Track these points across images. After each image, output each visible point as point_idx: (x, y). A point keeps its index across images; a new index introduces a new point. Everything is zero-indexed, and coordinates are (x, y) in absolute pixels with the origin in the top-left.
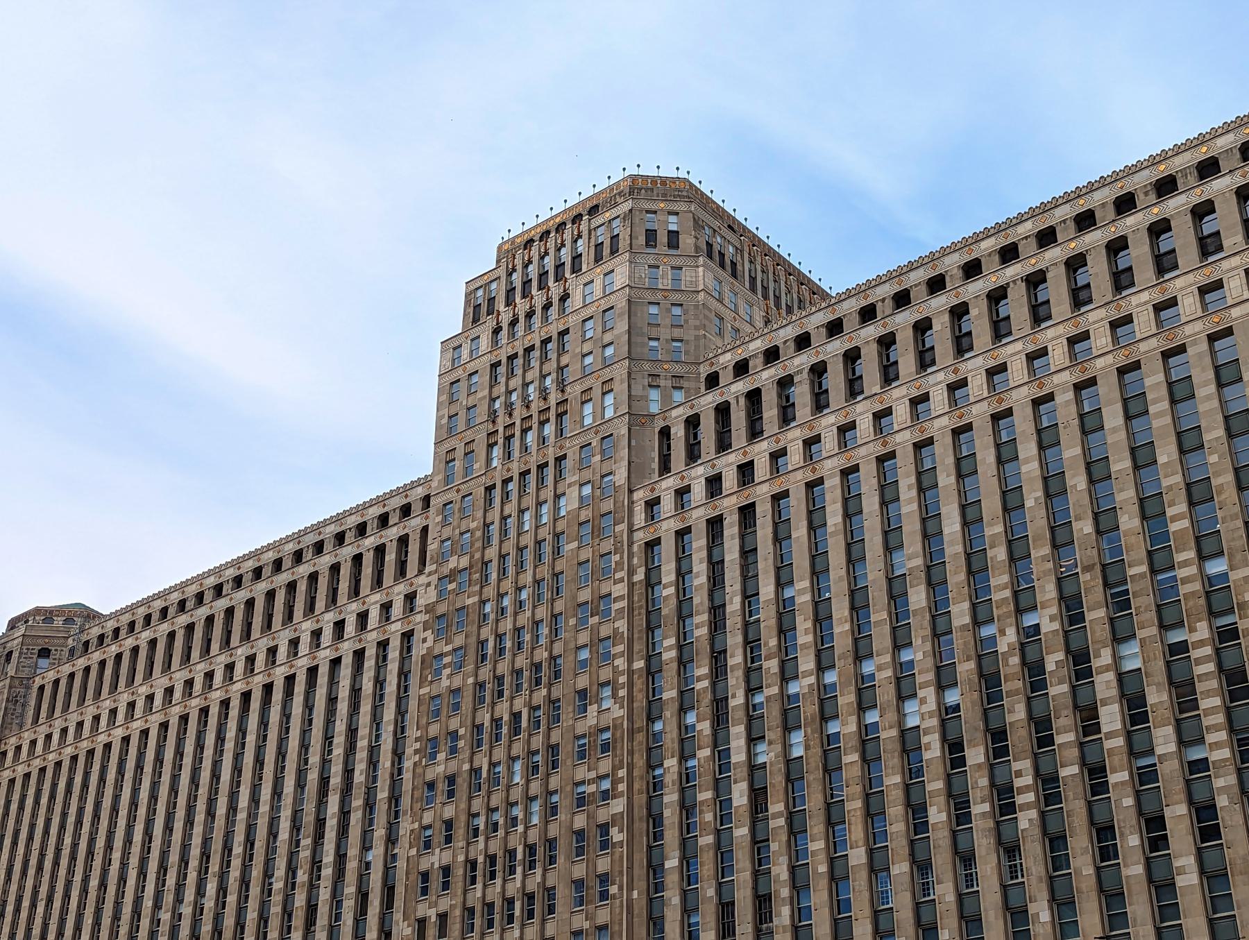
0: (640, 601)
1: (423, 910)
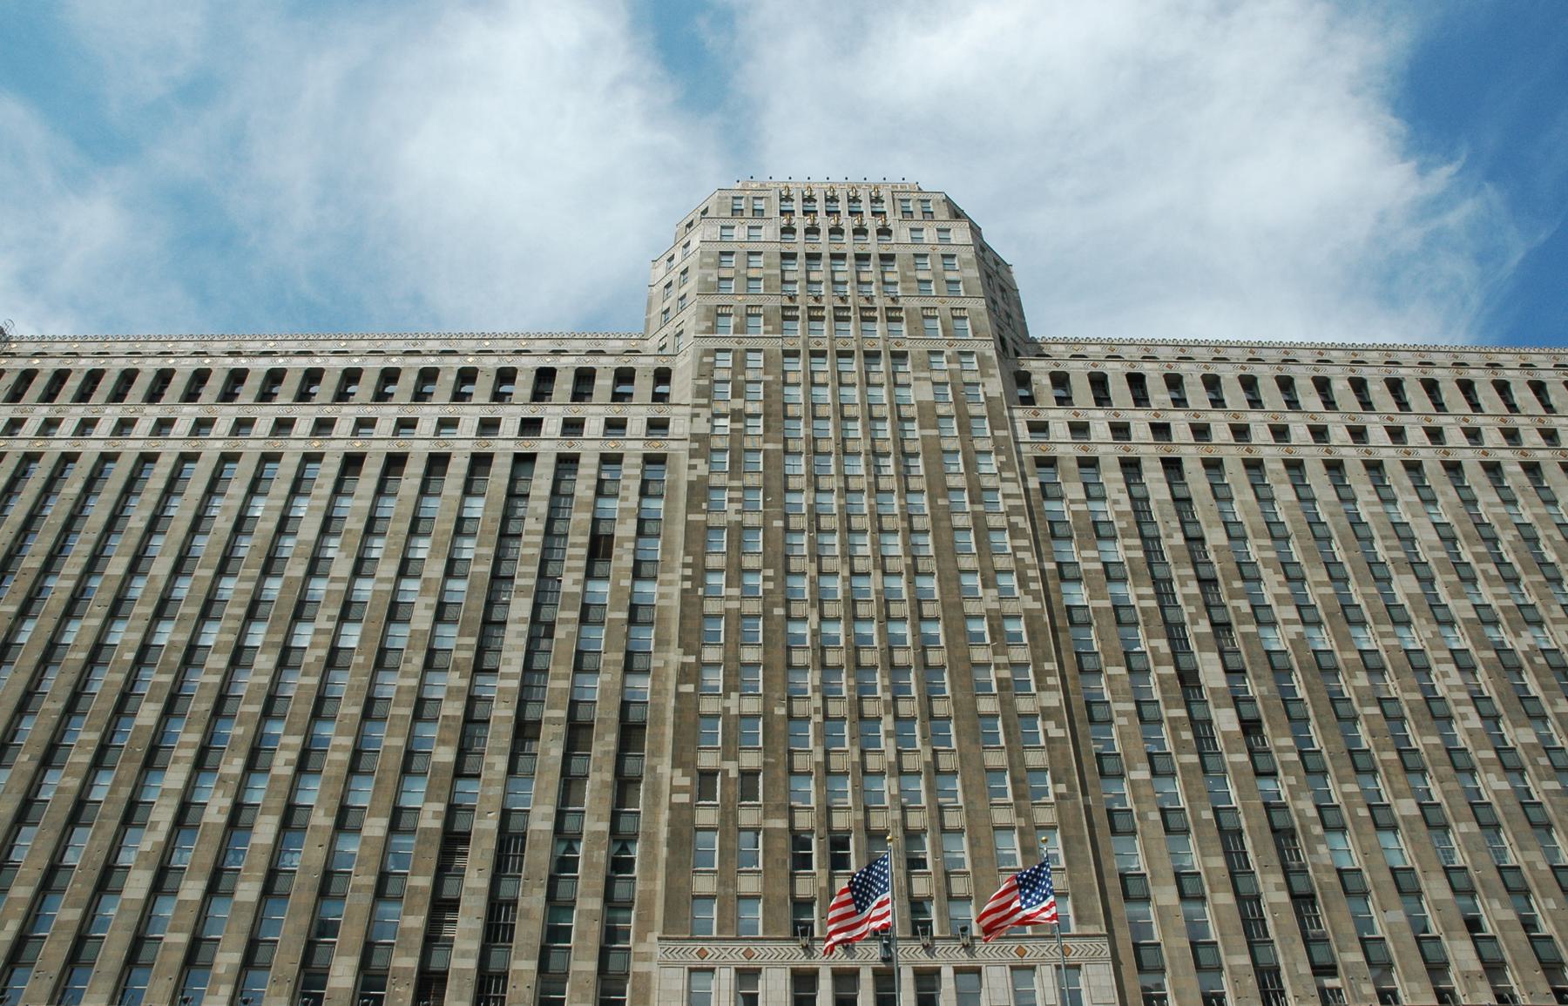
1: (707, 760)
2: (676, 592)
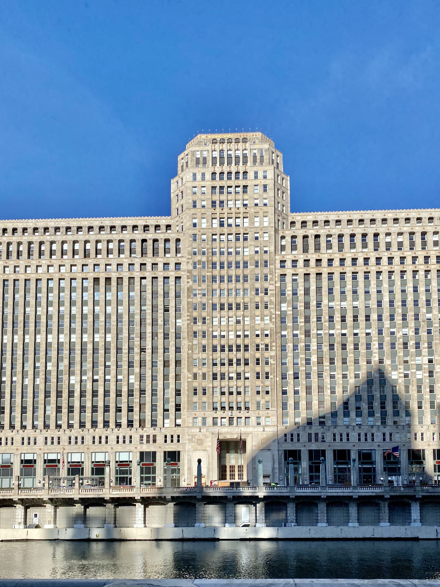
0: (278, 293)
1: (195, 370)
2: (186, 323)
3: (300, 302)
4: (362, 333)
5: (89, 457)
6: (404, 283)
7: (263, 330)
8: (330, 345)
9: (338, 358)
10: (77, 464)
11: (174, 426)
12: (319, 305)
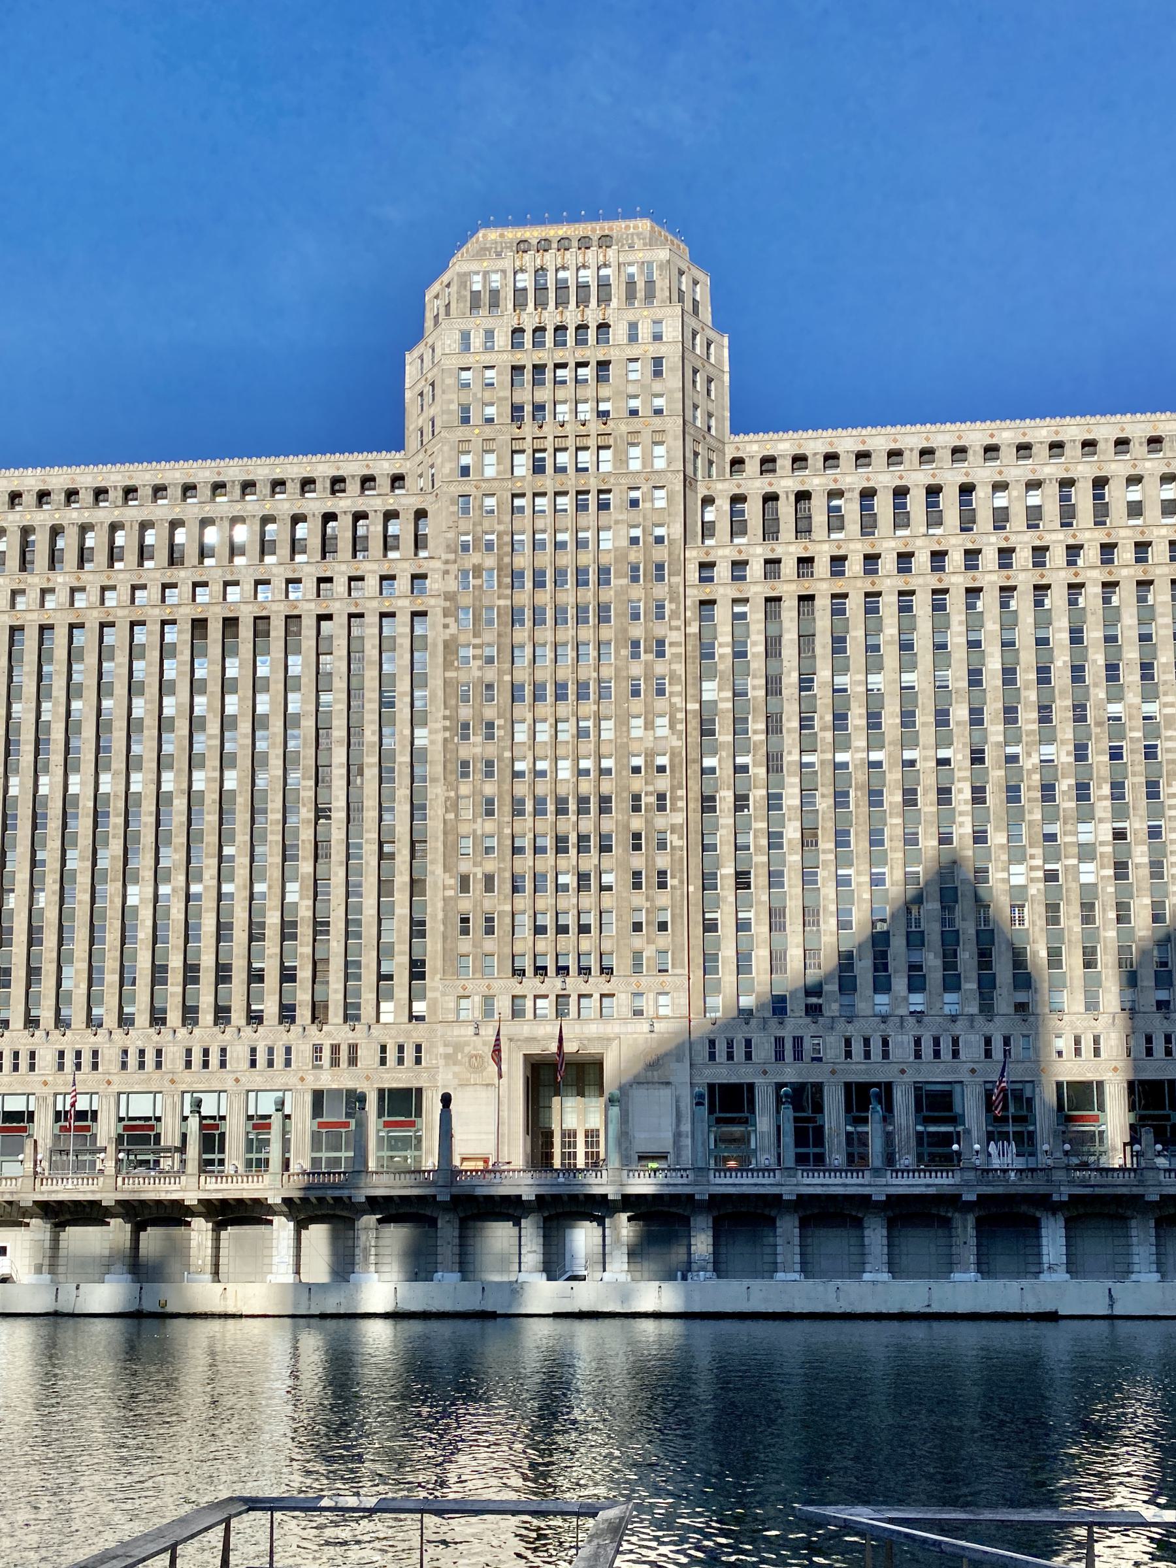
0: (693, 651)
1: (464, 867)
2: (439, 737)
3: (754, 677)
4: (925, 759)
5: (174, 1104)
6: (1043, 619)
7: (650, 755)
8: (836, 794)
9: (860, 829)
10: (142, 1123)
11: (407, 1020)
12: (806, 683)
